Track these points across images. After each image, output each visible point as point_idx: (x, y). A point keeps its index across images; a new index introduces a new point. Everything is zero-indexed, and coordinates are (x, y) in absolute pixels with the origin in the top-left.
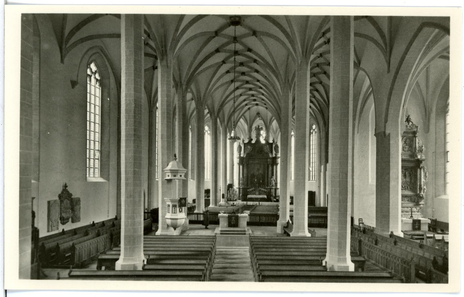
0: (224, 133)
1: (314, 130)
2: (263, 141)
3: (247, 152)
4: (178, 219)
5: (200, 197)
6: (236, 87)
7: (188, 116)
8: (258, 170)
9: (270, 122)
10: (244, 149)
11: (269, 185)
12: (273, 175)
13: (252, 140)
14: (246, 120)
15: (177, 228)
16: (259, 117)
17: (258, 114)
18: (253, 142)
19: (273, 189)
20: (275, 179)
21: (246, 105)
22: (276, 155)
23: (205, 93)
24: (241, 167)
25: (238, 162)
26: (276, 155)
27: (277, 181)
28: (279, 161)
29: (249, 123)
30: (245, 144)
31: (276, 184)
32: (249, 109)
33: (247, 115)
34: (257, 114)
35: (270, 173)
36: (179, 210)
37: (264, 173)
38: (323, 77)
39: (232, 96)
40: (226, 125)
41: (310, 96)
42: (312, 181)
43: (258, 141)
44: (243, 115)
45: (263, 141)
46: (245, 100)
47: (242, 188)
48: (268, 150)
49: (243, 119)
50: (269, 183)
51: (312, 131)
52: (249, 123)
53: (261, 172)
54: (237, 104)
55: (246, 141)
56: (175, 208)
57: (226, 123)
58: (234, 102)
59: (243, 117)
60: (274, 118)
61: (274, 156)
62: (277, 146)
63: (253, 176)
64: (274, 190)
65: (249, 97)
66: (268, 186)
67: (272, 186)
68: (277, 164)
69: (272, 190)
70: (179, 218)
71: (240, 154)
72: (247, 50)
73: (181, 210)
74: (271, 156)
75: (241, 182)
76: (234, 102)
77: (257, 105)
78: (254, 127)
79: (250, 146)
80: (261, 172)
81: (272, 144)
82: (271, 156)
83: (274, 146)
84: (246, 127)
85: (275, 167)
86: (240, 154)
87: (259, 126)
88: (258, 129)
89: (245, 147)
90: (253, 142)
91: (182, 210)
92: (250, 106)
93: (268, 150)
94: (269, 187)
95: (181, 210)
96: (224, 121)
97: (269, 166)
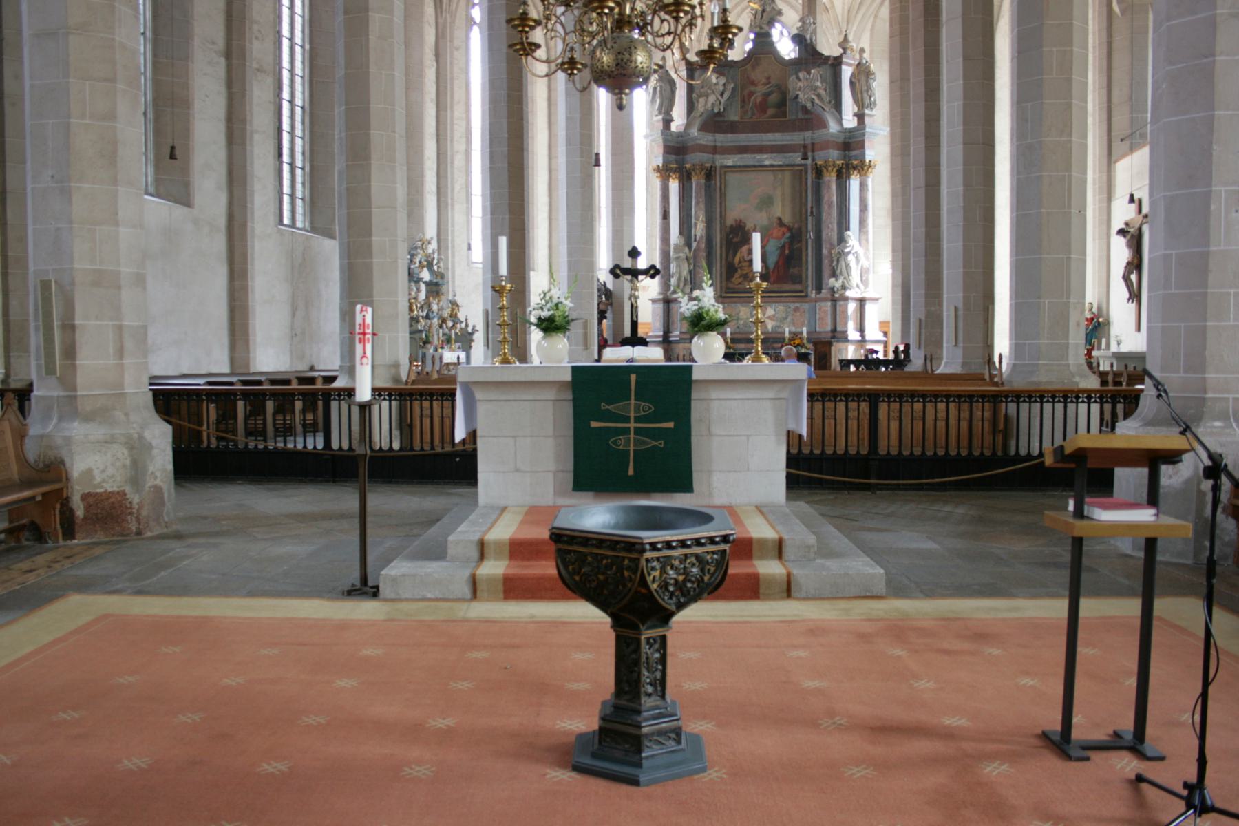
2: (786, 49)
5: (369, 268)
8: (767, 202)
10: (690, 89)
12: (843, 224)
18: (734, 55)
19: (847, 299)
22: (860, 117)
24: (674, 185)
25: (659, 161)
26: (860, 117)
30: (691, 67)
48: (822, 92)
50: (826, 271)
53: (779, 214)
61: (849, 121)
62: (863, 72)
64: (852, 307)
66: (819, 289)
68: (862, 167)
71: (667, 122)
82: (833, 127)
83: (847, 72)
85: (854, 183)
89: (691, 76)
90: (741, 48)
93: (822, 92)
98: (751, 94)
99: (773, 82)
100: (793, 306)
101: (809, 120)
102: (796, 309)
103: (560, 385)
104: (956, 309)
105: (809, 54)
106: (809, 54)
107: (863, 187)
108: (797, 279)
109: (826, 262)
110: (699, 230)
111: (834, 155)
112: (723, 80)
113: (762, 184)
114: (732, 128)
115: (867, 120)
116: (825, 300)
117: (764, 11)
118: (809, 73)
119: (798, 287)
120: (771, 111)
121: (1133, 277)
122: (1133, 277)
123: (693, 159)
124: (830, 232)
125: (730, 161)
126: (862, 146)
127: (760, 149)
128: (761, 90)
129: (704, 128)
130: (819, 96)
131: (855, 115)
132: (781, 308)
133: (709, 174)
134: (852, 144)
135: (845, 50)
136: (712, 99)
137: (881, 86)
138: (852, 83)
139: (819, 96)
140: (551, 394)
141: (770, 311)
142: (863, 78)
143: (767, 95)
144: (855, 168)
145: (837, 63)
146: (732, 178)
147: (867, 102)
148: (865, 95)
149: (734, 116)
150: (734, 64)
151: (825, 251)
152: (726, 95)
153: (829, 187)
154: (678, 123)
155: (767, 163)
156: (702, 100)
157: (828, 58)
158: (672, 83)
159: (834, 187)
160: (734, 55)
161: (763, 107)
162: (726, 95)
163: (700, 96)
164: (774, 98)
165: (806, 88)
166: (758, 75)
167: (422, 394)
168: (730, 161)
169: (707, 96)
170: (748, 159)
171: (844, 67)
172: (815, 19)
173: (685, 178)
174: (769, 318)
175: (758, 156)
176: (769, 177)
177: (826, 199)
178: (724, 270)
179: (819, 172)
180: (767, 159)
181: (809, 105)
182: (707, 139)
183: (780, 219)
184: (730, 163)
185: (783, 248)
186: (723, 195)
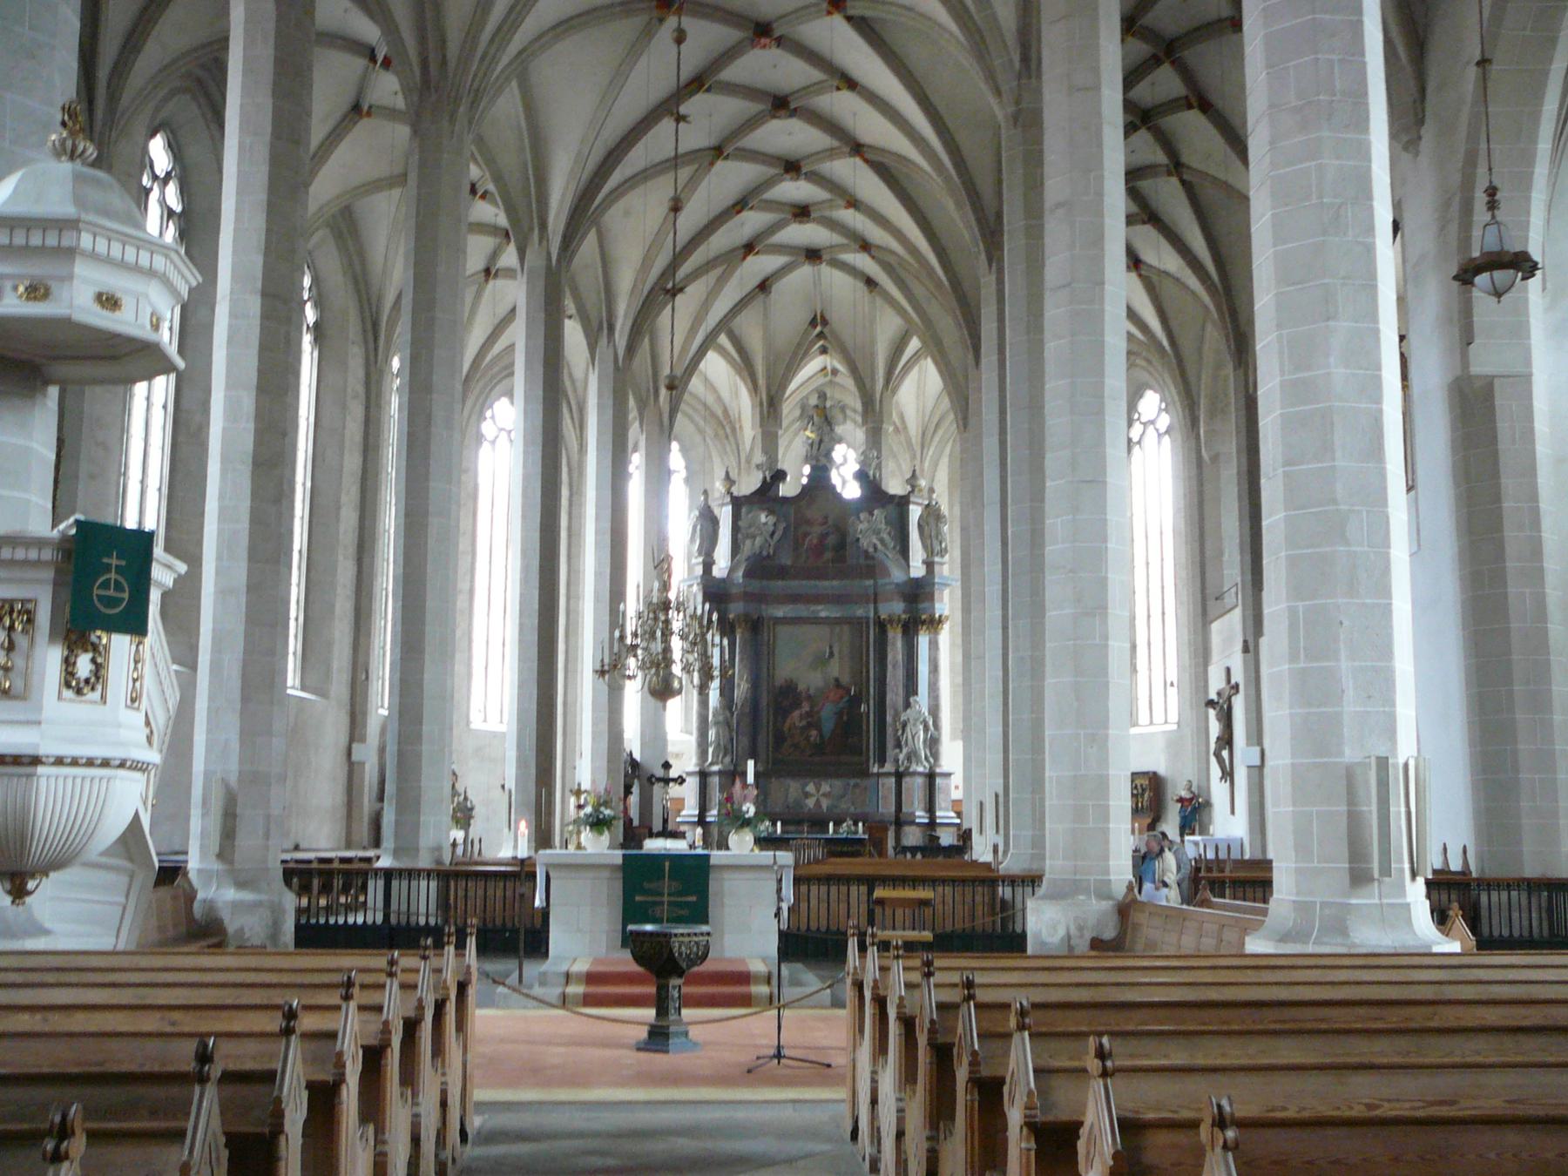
0: (609, 438)
1: (1152, 422)
3: (747, 548)
4: (36, 761)
6: (686, 75)
7: (380, 298)
9: (888, 381)
10: (736, 529)
11: (891, 752)
12: (911, 688)
13: (780, 476)
14: (745, 364)
15: (44, 871)
16: (824, 351)
17: (819, 321)
18: (787, 489)
19: (915, 773)
20: (925, 710)
21: (749, 248)
23: (471, 36)
26: (929, 565)
27: (936, 726)
28: (946, 603)
29: (761, 382)
30: (737, 503)
31: (933, 743)
32: (764, 286)
33: (750, 326)
34: (813, 323)
35: (895, 677)
36: (69, 664)
37: (860, 675)
38: (1192, 128)
39: (660, 141)
40: (621, 352)
41: (1131, 220)
42: (1152, 729)
43: (819, 483)
44: (724, 324)
45: (851, 491)
46: (740, 205)
47: (720, 773)
48: (885, 536)
49: (722, 351)
51: (1135, 433)
52: (761, 382)
53: (836, 673)
54: (689, 221)
55: (749, 484)
56: (21, 641)
57: (621, 339)
58: (676, 207)
59: (723, 339)
60: (914, 344)
61: (917, 570)
62: (932, 514)
63: (787, 696)
64: (920, 780)
65: (769, 183)
66: (882, 761)
67: (912, 756)
69: (906, 781)
70: (48, 748)
71: (708, 565)
72: (750, 34)
73: (84, 665)
74: (897, 575)
75: (712, 734)
76: (676, 207)
77: (813, 255)
78: (789, 409)
79: (771, 512)
80: (837, 669)
81: (902, 503)
83: (915, 512)
84: (744, 405)
85: (923, 640)
86: (708, 565)
87: (822, 396)
88: (823, 418)
91: (99, 669)
92: (778, 261)
93: (885, 536)
94: (889, 767)
95: (84, 665)
96: (611, 328)
97: (890, 634)
98: (806, 535)
99: (830, 522)
100: (852, 782)
101: (871, 567)
102: (856, 786)
103: (612, 867)
104: (997, 796)
105: (875, 493)
106: (875, 493)
107: (934, 646)
108: (858, 750)
109: (889, 730)
110: (741, 689)
111: (897, 607)
112: (772, 519)
113: (816, 639)
114: (782, 573)
115: (937, 568)
116: (888, 774)
117: (821, 441)
118: (871, 514)
119: (856, 759)
120: (828, 555)
121: (1225, 754)
122: (1225, 754)
123: (735, 609)
124: (894, 695)
125: (780, 612)
126: (931, 598)
127: (817, 599)
128: (817, 530)
129: (748, 574)
130: (882, 541)
131: (924, 562)
132: (838, 783)
133: (755, 626)
134: (918, 593)
135: (913, 487)
136: (758, 541)
137: (951, 533)
138: (920, 526)
139: (882, 541)
140: (606, 874)
141: (825, 788)
142: (932, 521)
143: (823, 536)
144: (923, 623)
145: (902, 503)
146: (783, 631)
147: (937, 548)
148: (935, 542)
149: (786, 560)
150: (785, 499)
151: (889, 719)
152: (776, 537)
153: (894, 644)
154: (722, 564)
155: (823, 614)
156: (748, 542)
157: (893, 497)
158: (714, 522)
159: (899, 644)
160: (787, 489)
161: (819, 549)
162: (776, 537)
163: (747, 536)
164: (831, 540)
165: (870, 531)
166: (813, 513)
167: (457, 875)
168: (780, 612)
169: (754, 537)
170: (802, 610)
171: (912, 507)
172: (879, 451)
173: (726, 628)
174: (824, 795)
175: (813, 608)
176: (824, 630)
177: (890, 657)
178: (771, 740)
179: (882, 626)
180: (823, 612)
181: (871, 550)
182: (755, 585)
183: (837, 680)
184: (780, 614)
185: (840, 714)
186: (772, 653)
